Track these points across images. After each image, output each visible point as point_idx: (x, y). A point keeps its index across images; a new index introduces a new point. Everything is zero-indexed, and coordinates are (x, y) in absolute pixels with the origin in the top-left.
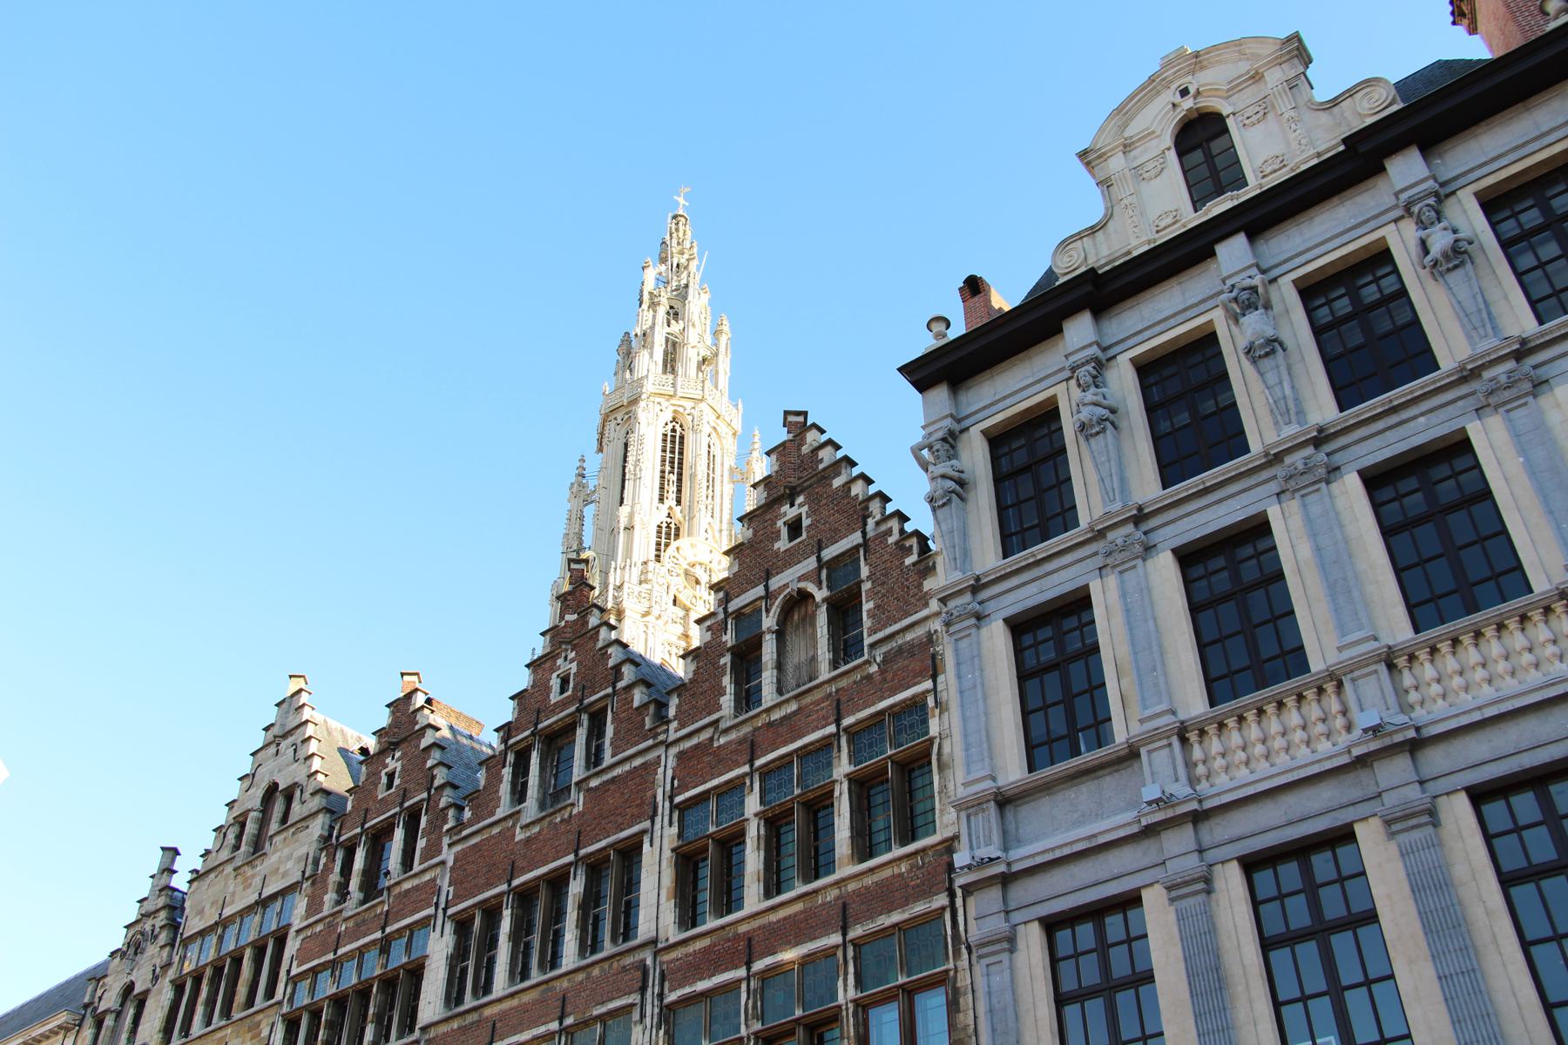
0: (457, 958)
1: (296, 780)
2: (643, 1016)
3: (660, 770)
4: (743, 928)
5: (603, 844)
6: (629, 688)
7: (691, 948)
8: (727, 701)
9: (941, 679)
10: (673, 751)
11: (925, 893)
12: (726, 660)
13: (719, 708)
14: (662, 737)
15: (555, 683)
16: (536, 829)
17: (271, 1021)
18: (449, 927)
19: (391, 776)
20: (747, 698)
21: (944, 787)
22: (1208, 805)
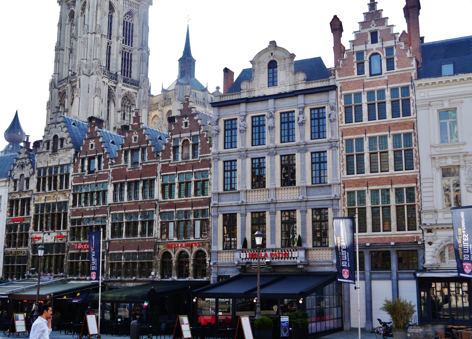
0: (115, 191)
1: (64, 137)
2: (156, 213)
3: (158, 167)
4: (175, 202)
5: (146, 178)
6: (151, 146)
7: (165, 203)
8: (172, 157)
9: (211, 168)
10: (161, 164)
11: (206, 205)
12: (171, 148)
13: (170, 158)
14: (158, 160)
15: (133, 138)
16: (131, 170)
17: (69, 193)
18: (112, 185)
19: (92, 145)
20: (175, 158)
21: (210, 188)
22: (248, 204)
